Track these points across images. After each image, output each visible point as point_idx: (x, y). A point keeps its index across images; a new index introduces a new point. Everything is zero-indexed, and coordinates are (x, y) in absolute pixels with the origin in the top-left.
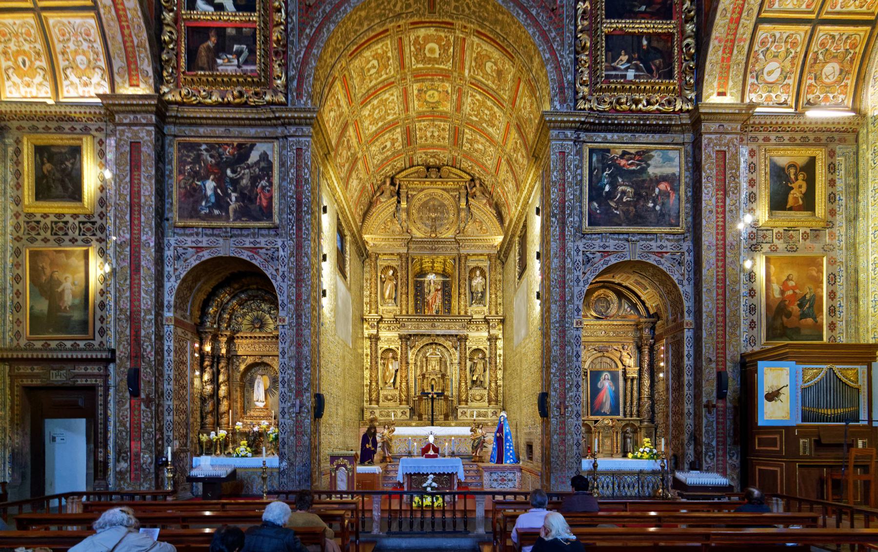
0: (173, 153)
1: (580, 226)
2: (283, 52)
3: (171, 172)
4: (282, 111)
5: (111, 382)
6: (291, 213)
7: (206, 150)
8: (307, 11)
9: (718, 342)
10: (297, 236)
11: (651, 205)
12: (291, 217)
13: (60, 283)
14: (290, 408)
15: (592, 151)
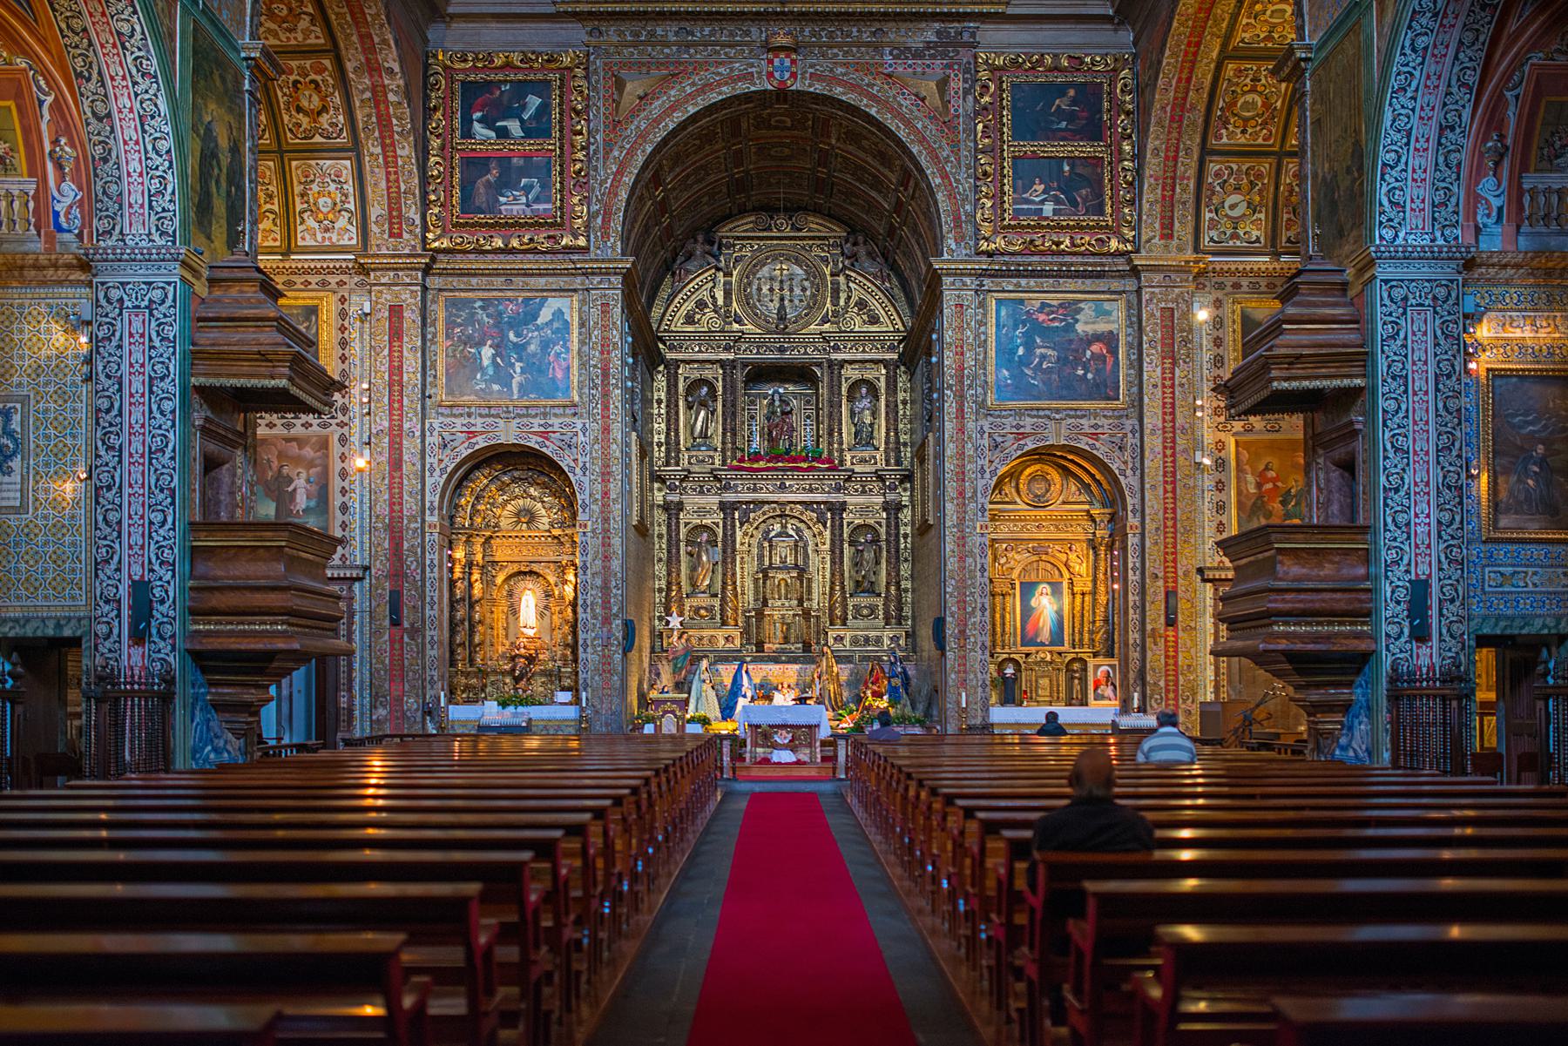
0: (439, 312)
1: (984, 400)
3: (435, 335)
4: (585, 261)
6: (595, 387)
7: (482, 308)
8: (614, 129)
9: (1166, 553)
10: (603, 417)
11: (1080, 372)
12: (594, 392)
14: (594, 639)
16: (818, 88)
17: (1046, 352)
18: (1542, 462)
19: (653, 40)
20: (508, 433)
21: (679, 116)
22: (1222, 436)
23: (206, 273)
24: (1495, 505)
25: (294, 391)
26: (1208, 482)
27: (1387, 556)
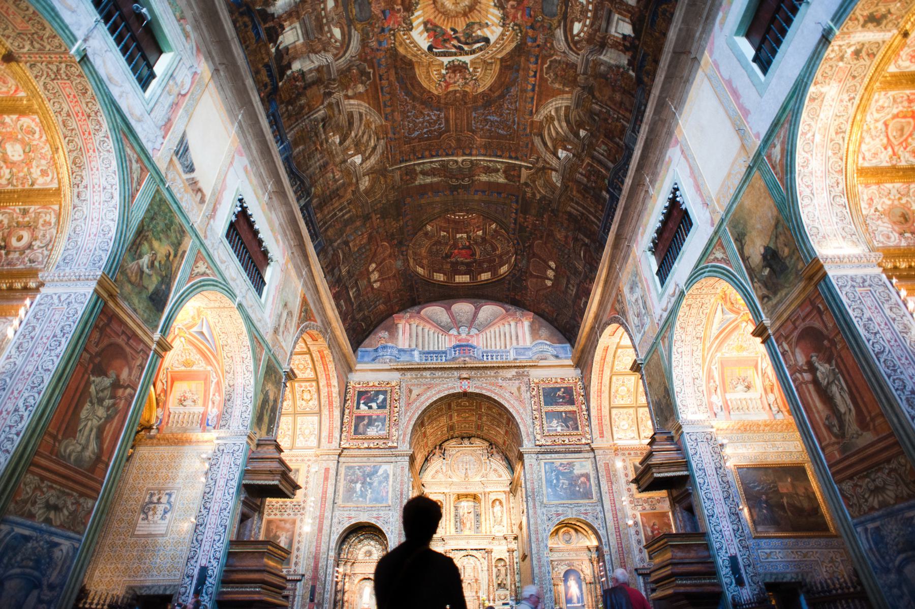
0: (342, 470)
2: (396, 424)
5: (297, 593)
13: (279, 537)
15: (545, 463)
16: (477, 391)
17: (564, 482)
18: (766, 502)
19: (422, 376)
20: (364, 518)
21: (430, 401)
22: (634, 512)
23: (256, 442)
24: (754, 522)
25: (281, 486)
26: (632, 531)
27: (716, 546)
